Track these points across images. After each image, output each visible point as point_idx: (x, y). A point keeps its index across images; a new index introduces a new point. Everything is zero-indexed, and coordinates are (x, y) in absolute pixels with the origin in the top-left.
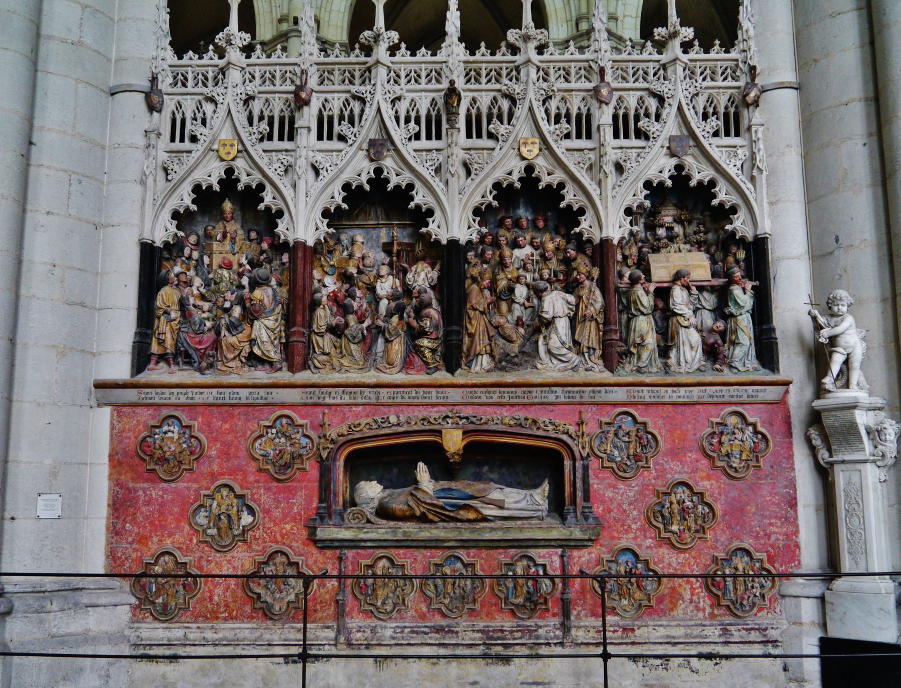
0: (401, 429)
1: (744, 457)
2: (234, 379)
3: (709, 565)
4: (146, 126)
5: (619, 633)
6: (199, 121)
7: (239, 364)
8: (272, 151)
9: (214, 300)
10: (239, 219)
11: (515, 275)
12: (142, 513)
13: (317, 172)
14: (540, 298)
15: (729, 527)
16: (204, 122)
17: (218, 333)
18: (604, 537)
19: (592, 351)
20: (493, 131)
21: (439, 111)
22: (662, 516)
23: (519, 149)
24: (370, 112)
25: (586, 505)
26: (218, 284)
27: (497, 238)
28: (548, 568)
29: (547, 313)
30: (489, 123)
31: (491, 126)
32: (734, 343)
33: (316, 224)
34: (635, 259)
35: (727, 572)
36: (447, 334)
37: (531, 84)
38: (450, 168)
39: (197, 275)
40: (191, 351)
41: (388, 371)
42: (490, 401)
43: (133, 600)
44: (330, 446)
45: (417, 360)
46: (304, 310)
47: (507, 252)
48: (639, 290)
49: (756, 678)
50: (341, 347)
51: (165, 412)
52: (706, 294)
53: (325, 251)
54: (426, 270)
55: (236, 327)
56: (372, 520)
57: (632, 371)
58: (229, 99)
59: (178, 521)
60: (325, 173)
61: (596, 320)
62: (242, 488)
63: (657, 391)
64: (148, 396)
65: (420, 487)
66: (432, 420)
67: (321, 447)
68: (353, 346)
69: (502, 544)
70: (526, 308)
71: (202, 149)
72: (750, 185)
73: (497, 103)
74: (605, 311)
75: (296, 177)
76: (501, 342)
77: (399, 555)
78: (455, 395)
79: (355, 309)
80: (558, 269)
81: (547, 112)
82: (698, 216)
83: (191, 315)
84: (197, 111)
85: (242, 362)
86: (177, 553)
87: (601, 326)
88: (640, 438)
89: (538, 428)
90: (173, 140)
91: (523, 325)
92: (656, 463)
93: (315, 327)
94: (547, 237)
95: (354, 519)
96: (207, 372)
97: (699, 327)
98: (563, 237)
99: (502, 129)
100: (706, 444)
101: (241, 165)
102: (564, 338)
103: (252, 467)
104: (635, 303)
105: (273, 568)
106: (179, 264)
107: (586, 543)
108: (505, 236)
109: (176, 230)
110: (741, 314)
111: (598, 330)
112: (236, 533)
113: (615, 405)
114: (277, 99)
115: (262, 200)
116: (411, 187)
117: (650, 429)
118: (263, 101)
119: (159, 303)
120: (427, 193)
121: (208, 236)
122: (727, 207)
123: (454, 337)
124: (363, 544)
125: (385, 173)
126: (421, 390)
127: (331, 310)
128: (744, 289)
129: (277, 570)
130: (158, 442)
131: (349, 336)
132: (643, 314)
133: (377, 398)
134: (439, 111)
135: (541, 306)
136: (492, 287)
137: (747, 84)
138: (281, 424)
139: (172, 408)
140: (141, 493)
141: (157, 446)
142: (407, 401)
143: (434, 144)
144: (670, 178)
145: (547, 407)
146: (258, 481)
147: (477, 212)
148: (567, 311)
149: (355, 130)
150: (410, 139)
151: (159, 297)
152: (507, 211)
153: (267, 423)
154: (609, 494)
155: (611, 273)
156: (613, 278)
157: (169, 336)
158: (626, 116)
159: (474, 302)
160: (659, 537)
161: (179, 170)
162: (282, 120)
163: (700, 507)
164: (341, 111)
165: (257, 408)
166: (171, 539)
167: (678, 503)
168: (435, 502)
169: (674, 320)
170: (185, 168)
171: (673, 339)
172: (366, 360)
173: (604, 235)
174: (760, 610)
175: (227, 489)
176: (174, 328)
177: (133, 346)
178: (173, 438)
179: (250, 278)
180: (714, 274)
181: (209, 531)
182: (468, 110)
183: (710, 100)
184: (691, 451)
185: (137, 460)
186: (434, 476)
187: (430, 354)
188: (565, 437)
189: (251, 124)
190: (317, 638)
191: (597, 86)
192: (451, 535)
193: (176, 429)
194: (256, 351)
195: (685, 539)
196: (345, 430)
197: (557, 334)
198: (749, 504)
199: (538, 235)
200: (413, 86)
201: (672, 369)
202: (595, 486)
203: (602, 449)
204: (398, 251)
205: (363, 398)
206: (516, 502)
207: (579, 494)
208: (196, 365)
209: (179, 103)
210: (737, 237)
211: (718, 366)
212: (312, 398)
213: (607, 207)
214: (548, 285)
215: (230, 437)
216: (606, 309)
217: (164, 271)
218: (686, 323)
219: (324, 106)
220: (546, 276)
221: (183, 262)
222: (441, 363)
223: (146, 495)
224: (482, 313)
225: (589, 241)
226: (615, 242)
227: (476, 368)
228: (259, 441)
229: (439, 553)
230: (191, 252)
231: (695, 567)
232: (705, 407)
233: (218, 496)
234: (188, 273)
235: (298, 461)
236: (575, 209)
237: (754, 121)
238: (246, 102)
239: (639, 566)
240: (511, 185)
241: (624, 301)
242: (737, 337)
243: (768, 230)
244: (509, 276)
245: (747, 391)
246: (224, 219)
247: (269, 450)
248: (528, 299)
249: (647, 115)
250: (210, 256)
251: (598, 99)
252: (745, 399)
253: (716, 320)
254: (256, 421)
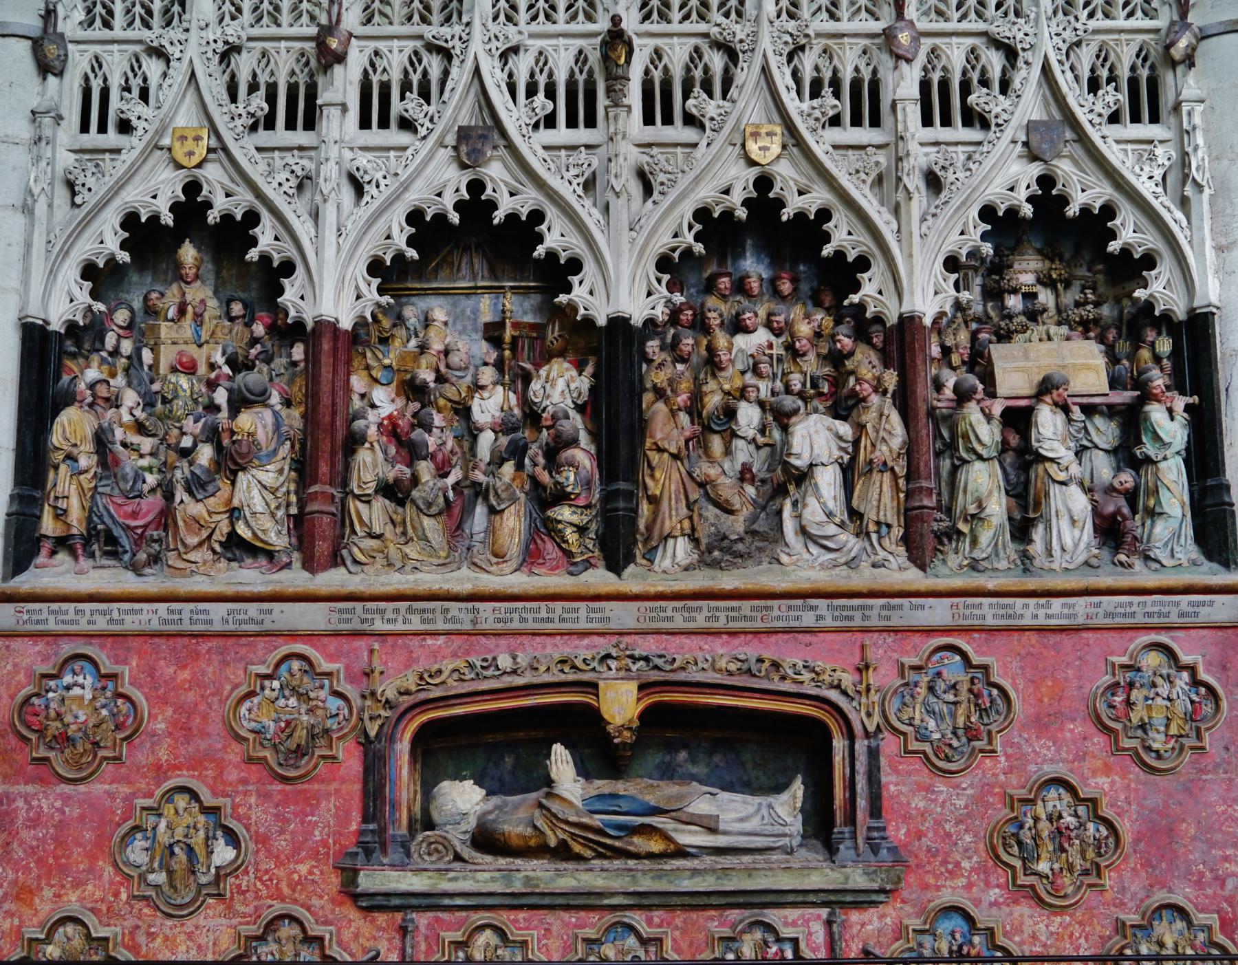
0: (519, 681)
1: (1173, 730)
2: (199, 585)
3: (1110, 938)
4: (34, 103)
6: (136, 92)
7: (209, 556)
8: (273, 149)
9: (161, 433)
10: (211, 277)
11: (738, 383)
12: (22, 842)
13: (358, 188)
14: (785, 429)
15: (1147, 864)
16: (144, 95)
17: (169, 496)
18: (909, 885)
19: (884, 530)
20: (694, 111)
21: (591, 72)
22: (1020, 843)
23: (743, 146)
24: (461, 76)
25: (874, 823)
26: (170, 401)
27: (703, 313)
28: (802, 945)
29: (798, 456)
30: (686, 96)
31: (691, 102)
32: (1153, 514)
33: (357, 287)
34: (966, 353)
35: (1144, 950)
36: (608, 497)
37: (766, 24)
38: (613, 181)
39: (129, 384)
40: (117, 532)
41: (494, 569)
42: (691, 625)
44: (384, 713)
45: (550, 548)
46: (333, 453)
47: (721, 339)
48: (973, 412)
50: (404, 522)
51: (67, 648)
52: (1099, 421)
53: (374, 340)
54: (567, 375)
55: (203, 485)
56: (466, 856)
57: (961, 567)
58: (192, 51)
59: (93, 858)
60: (374, 192)
61: (892, 469)
62: (215, 794)
63: (1012, 606)
64: (34, 617)
65: (556, 791)
66: (579, 663)
67: (366, 716)
68: (427, 522)
69: (714, 900)
70: (758, 448)
71: (140, 146)
72: (1179, 215)
73: (700, 58)
74: (908, 452)
75: (318, 198)
76: (711, 512)
77: (517, 923)
78: (623, 615)
79: (431, 449)
80: (818, 373)
81: (795, 74)
82: (1083, 272)
83: (117, 462)
84: (130, 75)
85: (214, 552)
86: (90, 920)
87: (901, 482)
88: (977, 696)
89: (783, 678)
90: (85, 128)
91: (752, 481)
92: (1004, 744)
93: (354, 485)
94: (797, 311)
95: (430, 854)
96: (148, 571)
97: (1087, 483)
98: (828, 310)
99: (711, 108)
100: (1101, 706)
101: (214, 176)
102: (831, 505)
103: (234, 754)
104: (966, 437)
105: (274, 947)
106: (95, 364)
107: (874, 897)
108: (717, 309)
109: (89, 300)
110: (1165, 459)
111: (898, 490)
112: (204, 880)
113: (929, 632)
114: (283, 52)
115: (254, 242)
116: (537, 216)
117: (995, 678)
118: (257, 55)
119: (56, 439)
120: (569, 228)
121: (151, 311)
122: (1137, 256)
123: (621, 504)
124: (447, 902)
125: (489, 191)
126: (558, 605)
127: (385, 452)
128: (1170, 411)
129: (282, 952)
130: (53, 705)
131: (420, 503)
132: (980, 457)
133: (474, 622)
134: (591, 72)
135: (786, 443)
136: (694, 408)
137: (1173, 23)
138: (290, 670)
139: (82, 641)
140: (20, 803)
141: (53, 714)
142: (531, 625)
143: (582, 135)
144: (1029, 200)
145: (800, 636)
146: (244, 781)
147: (664, 263)
148: (836, 453)
149: (432, 109)
150: (536, 126)
151: (57, 428)
152: (722, 262)
153: (263, 670)
154: (918, 802)
155: (920, 380)
156: (924, 390)
157: (75, 502)
158: (944, 84)
159: (659, 435)
160: (1014, 884)
161: (95, 186)
162: (292, 90)
163: (1091, 826)
164: (406, 72)
165: (244, 641)
166: (78, 892)
167: (1050, 818)
168: (585, 820)
169: (1040, 468)
170: (109, 181)
171: (1037, 505)
172: (452, 548)
173: (905, 308)
175: (187, 797)
176: (86, 486)
177: (8, 523)
178: (82, 698)
179: (230, 391)
180: (1114, 383)
181: (151, 877)
182: (647, 72)
183: (1103, 55)
184: (1073, 720)
185: (13, 741)
186: (584, 771)
187: (576, 536)
188: (834, 695)
189: (233, 98)
191: (889, 28)
192: (617, 884)
193: (89, 681)
194: (242, 530)
195: (1063, 887)
196: (411, 683)
197: (818, 497)
198: (1184, 820)
199: (781, 307)
200: (541, 26)
201: (1037, 563)
202: (892, 788)
203: (905, 717)
204: (514, 339)
205: (446, 620)
206: (741, 820)
207: (862, 803)
208: (126, 557)
209: (97, 58)
210: (1157, 313)
211: (1122, 557)
212: (349, 621)
213: (911, 256)
214: (800, 403)
215: (191, 696)
216: (910, 450)
217: (66, 378)
218: (1062, 476)
219: (372, 64)
220: (797, 387)
221: (103, 360)
222: (597, 553)
223: (31, 808)
224: (675, 457)
225: (878, 319)
226: (928, 321)
227: (663, 562)
228: (247, 704)
229: (594, 917)
230: (118, 341)
231: (1082, 941)
232: (1098, 635)
233: (168, 810)
234: (112, 382)
235: (323, 742)
236: (850, 259)
237: (1185, 94)
238: (225, 57)
239: (976, 939)
240: (728, 214)
241: (945, 434)
242: (1159, 502)
243: (1214, 299)
244: (727, 387)
245: (1178, 604)
246: (182, 278)
247: (266, 721)
248: (763, 430)
249: (985, 82)
250: (155, 349)
251: (891, 52)
252: (1174, 619)
253: (1118, 469)
254: (242, 665)
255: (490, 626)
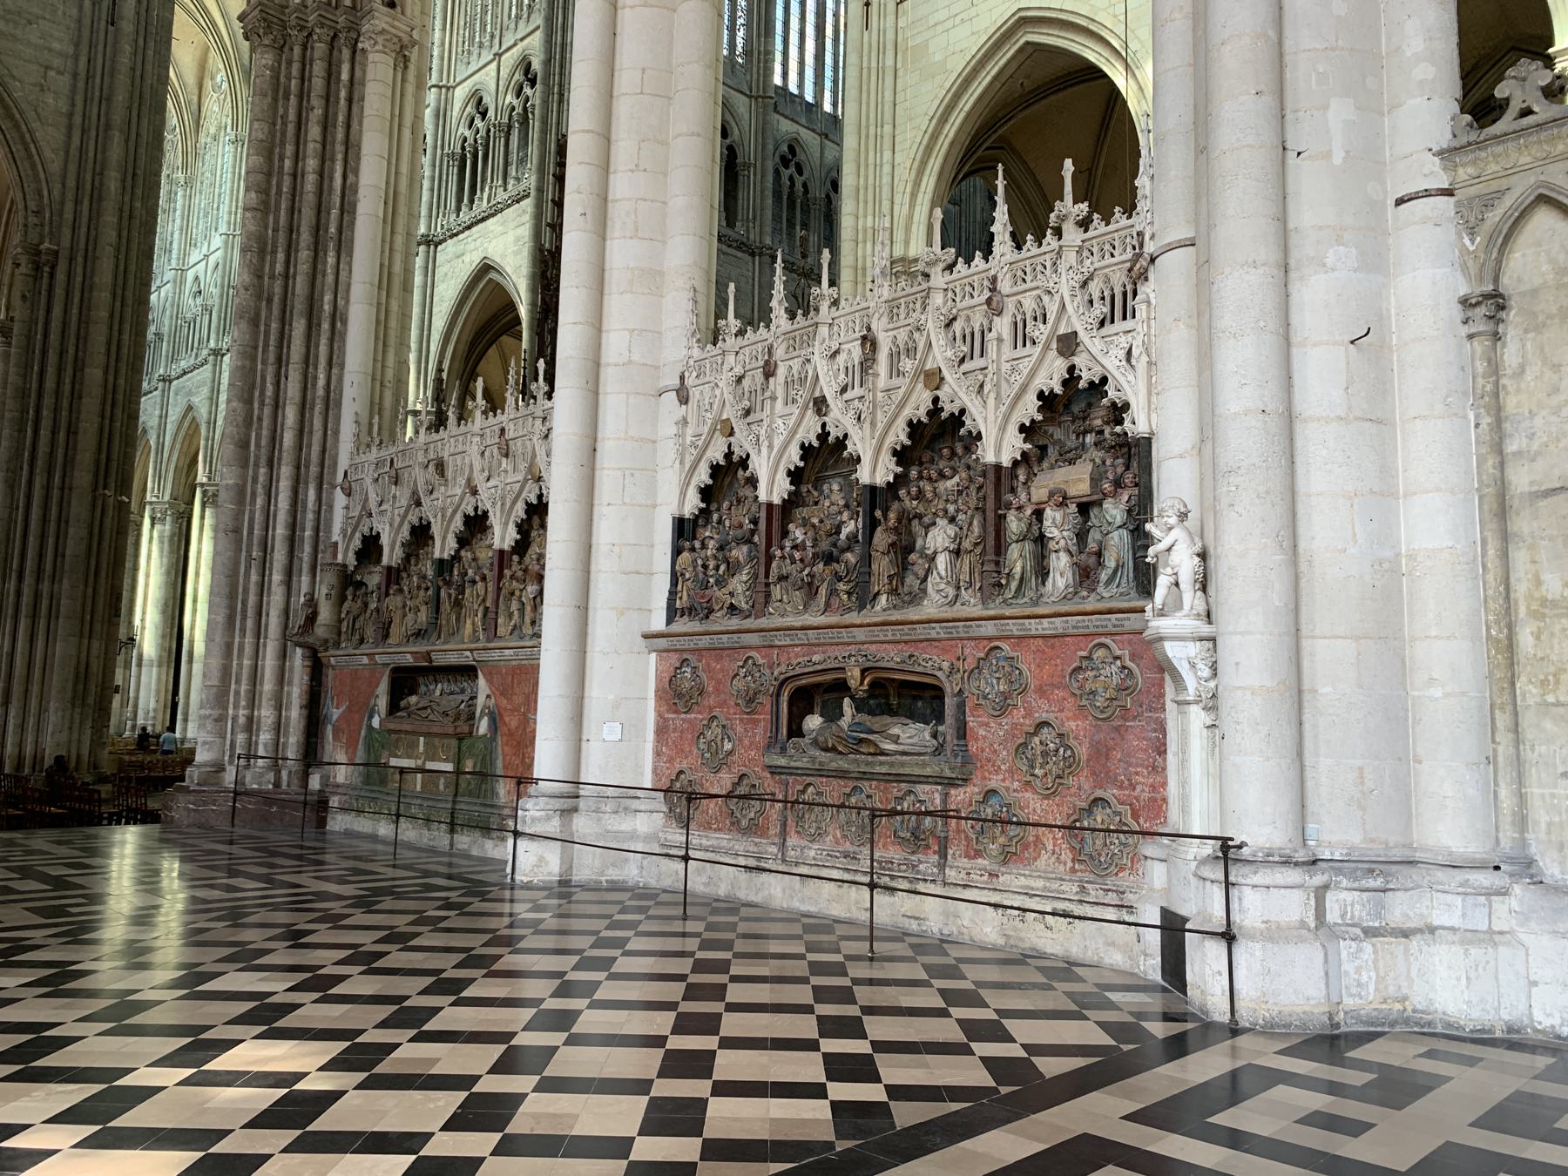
5: (985, 878)
15: (1094, 773)
43: (665, 809)
49: (1108, 945)
78: (860, 634)
92: (1023, 702)
113: (990, 639)
142: (828, 641)
154: (982, 732)
167: (1041, 743)
174: (1122, 869)
190: (766, 853)
215: (721, 676)
252: (1111, 629)
255: (814, 641)
